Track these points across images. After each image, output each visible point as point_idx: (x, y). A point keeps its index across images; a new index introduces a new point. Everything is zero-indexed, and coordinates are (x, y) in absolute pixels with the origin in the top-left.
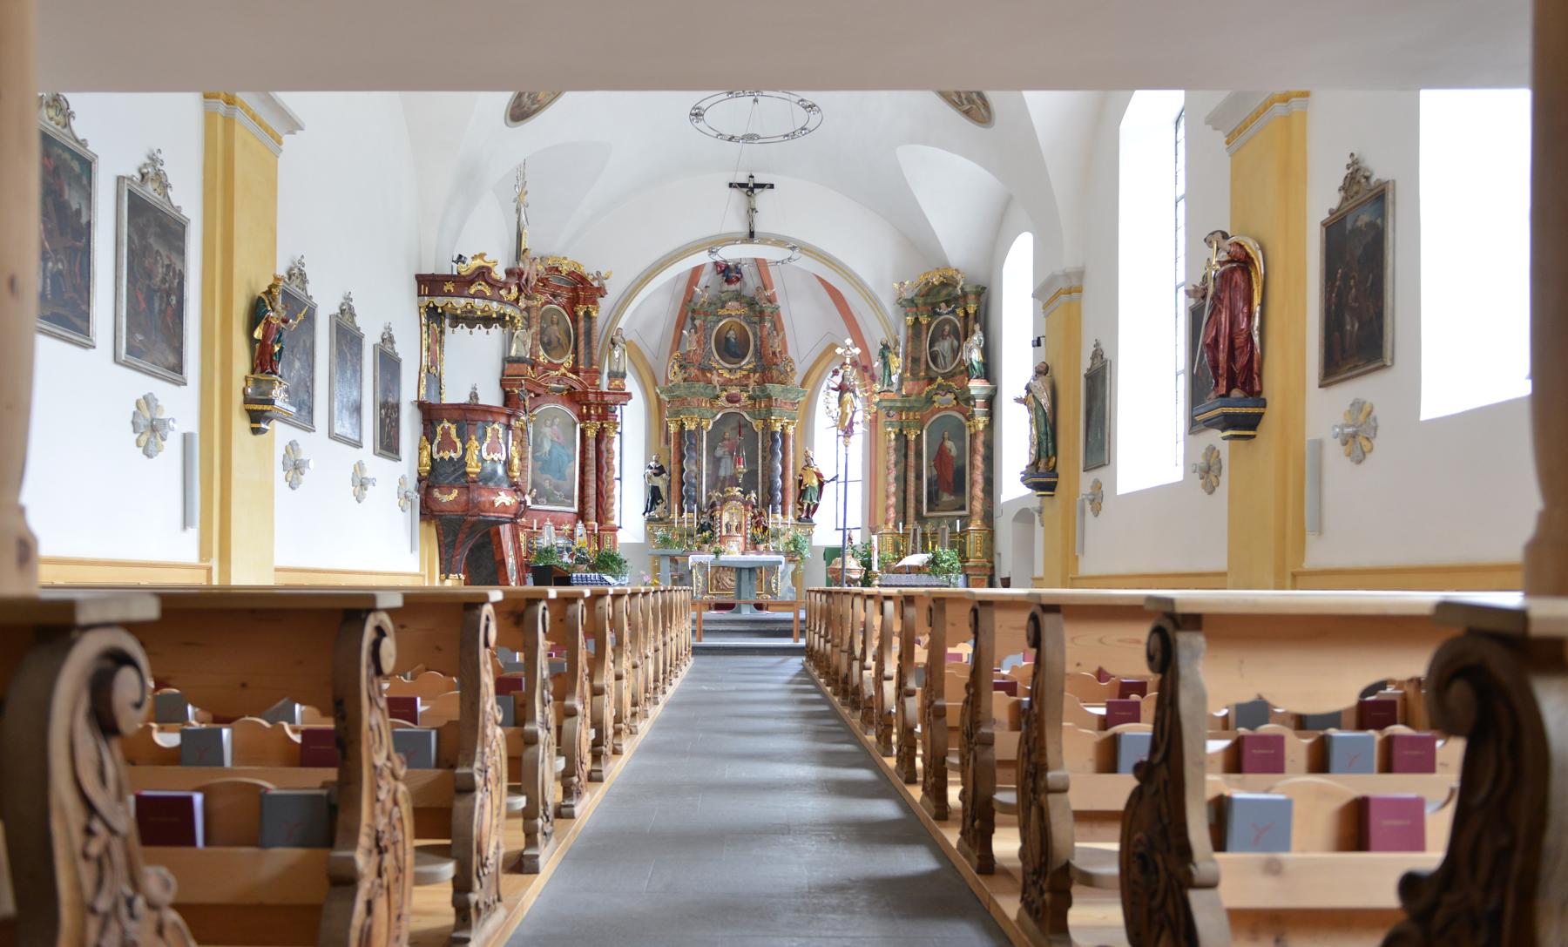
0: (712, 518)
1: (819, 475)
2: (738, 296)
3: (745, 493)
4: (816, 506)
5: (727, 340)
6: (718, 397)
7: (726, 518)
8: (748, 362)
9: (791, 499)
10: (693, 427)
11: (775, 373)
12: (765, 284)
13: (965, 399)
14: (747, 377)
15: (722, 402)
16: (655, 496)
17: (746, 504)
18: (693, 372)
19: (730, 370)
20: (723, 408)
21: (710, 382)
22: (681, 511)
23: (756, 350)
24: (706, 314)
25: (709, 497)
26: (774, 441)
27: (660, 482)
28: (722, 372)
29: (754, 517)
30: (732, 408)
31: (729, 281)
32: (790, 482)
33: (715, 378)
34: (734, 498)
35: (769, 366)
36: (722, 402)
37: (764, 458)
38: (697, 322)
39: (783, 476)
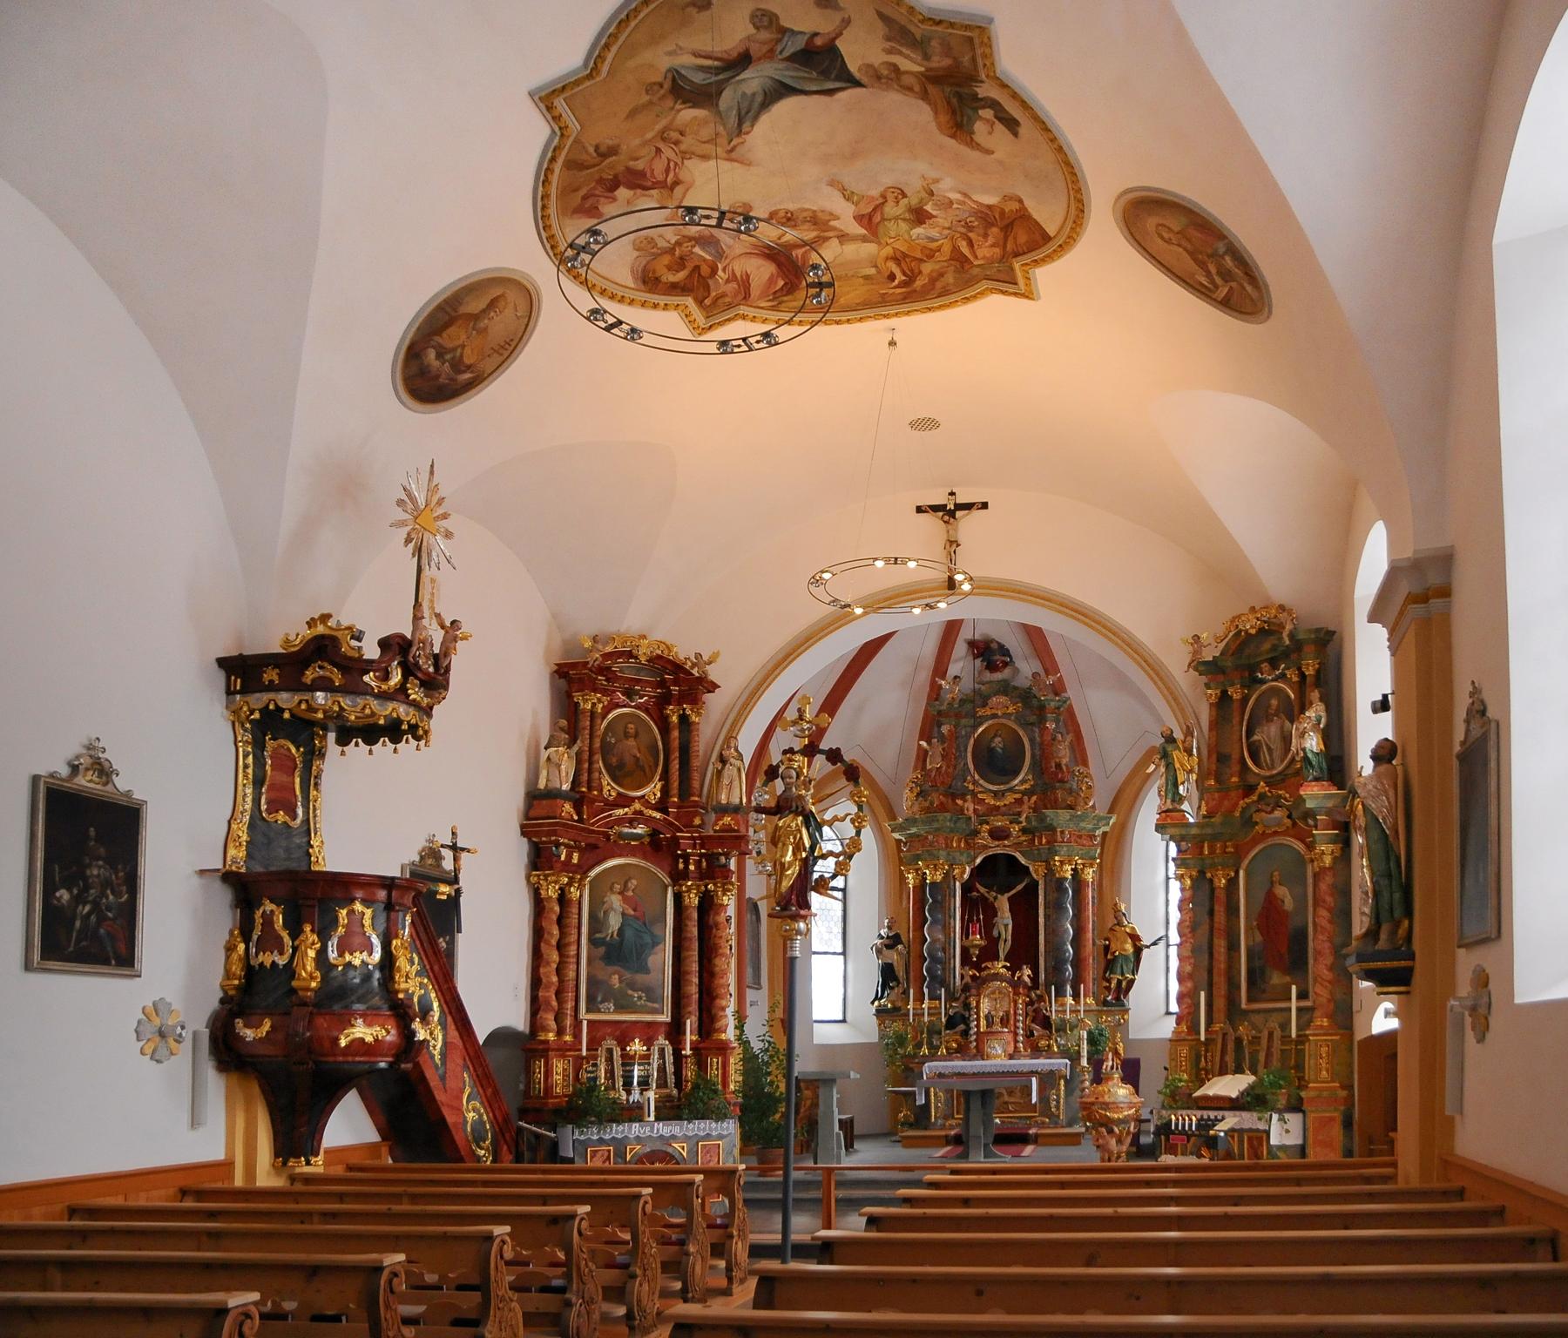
1: (1135, 938)
2: (1005, 688)
3: (1013, 969)
5: (991, 750)
6: (976, 833)
8: (1022, 780)
10: (939, 878)
11: (1059, 794)
15: (984, 838)
17: (1016, 985)
20: (986, 847)
21: (961, 810)
22: (920, 998)
24: (958, 716)
25: (962, 977)
26: (1062, 890)
29: (1031, 1003)
30: (997, 848)
31: (992, 667)
33: (970, 806)
34: (997, 977)
36: (984, 838)
37: (1047, 917)
38: (945, 729)
39: (1077, 941)
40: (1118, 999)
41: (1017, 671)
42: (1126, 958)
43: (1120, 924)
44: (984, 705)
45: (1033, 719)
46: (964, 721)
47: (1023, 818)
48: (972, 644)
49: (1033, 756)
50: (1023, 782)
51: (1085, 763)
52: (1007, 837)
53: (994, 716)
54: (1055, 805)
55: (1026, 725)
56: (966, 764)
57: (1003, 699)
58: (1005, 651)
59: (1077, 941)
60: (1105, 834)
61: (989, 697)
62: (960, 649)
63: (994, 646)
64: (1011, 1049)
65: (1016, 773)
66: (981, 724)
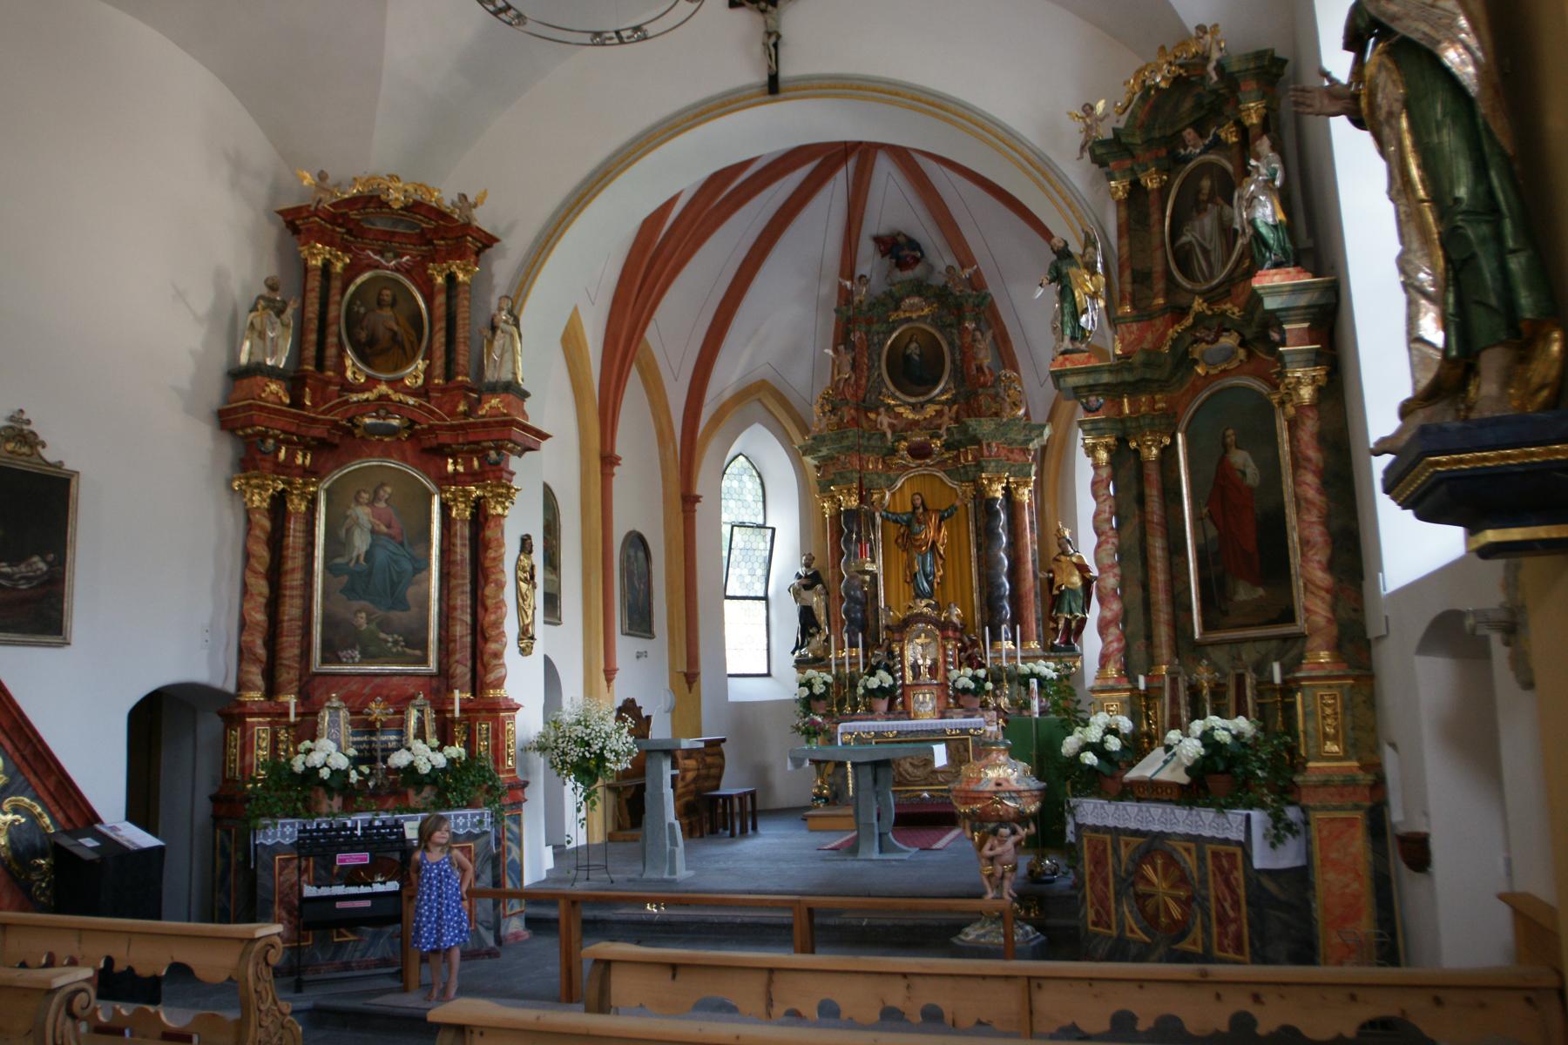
0: (890, 653)
5: (907, 358)
6: (893, 451)
8: (941, 390)
9: (1032, 613)
11: (983, 400)
12: (966, 258)
13: (1261, 331)
16: (808, 620)
17: (944, 626)
18: (848, 413)
19: (914, 407)
24: (869, 322)
27: (815, 600)
31: (902, 264)
32: (1029, 581)
33: (884, 420)
39: (1015, 573)
41: (931, 269)
42: (1073, 591)
43: (1064, 552)
44: (897, 308)
46: (875, 327)
47: (943, 431)
48: (877, 240)
49: (953, 361)
50: (942, 393)
51: (1015, 368)
53: (909, 320)
54: (978, 413)
55: (942, 328)
56: (880, 375)
57: (916, 300)
58: (914, 245)
59: (1015, 573)
60: (1044, 449)
61: (902, 299)
62: (866, 248)
63: (901, 239)
65: (936, 383)
66: (894, 329)
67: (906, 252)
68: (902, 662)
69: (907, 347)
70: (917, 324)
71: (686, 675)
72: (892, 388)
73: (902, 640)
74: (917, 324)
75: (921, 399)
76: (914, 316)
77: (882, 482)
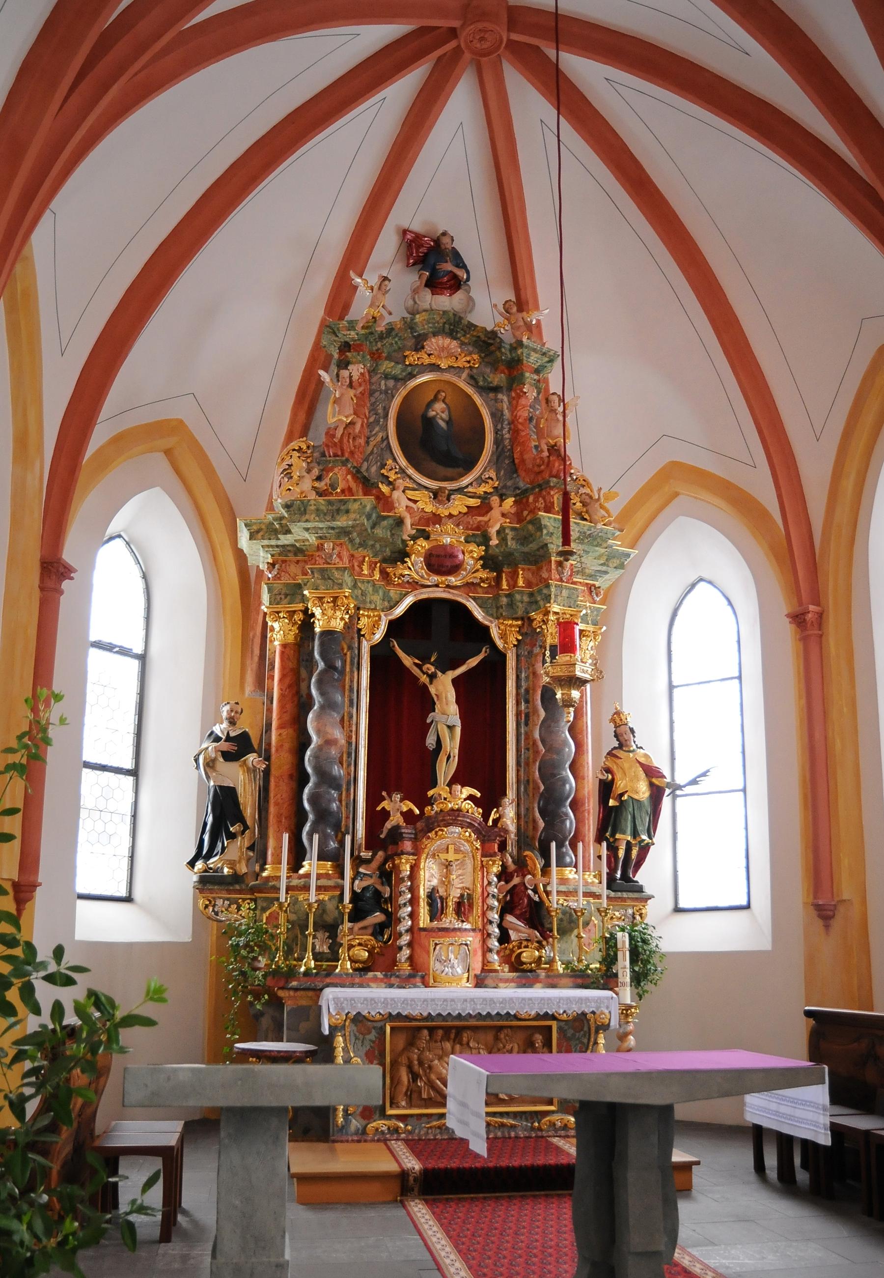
0: (387, 875)
1: (651, 772)
2: (455, 326)
4: (644, 850)
5: (429, 423)
6: (401, 555)
7: (430, 875)
8: (480, 477)
10: (338, 625)
14: (485, 507)
15: (415, 566)
16: (224, 808)
18: (341, 477)
20: (415, 585)
23: (498, 459)
24: (376, 356)
28: (411, 494)
29: (504, 875)
30: (437, 588)
31: (434, 284)
34: (454, 817)
35: (540, 478)
36: (415, 566)
37: (525, 719)
40: (625, 877)
45: (498, 379)
49: (498, 442)
50: (480, 481)
52: (454, 569)
62: (386, 247)
64: (477, 967)
65: (469, 465)
66: (412, 376)
67: (449, 267)
68: (413, 890)
69: (429, 405)
70: (447, 376)
71: (16, 886)
72: (403, 462)
73: (417, 852)
74: (447, 376)
75: (449, 486)
76: (443, 366)
77: (377, 598)
